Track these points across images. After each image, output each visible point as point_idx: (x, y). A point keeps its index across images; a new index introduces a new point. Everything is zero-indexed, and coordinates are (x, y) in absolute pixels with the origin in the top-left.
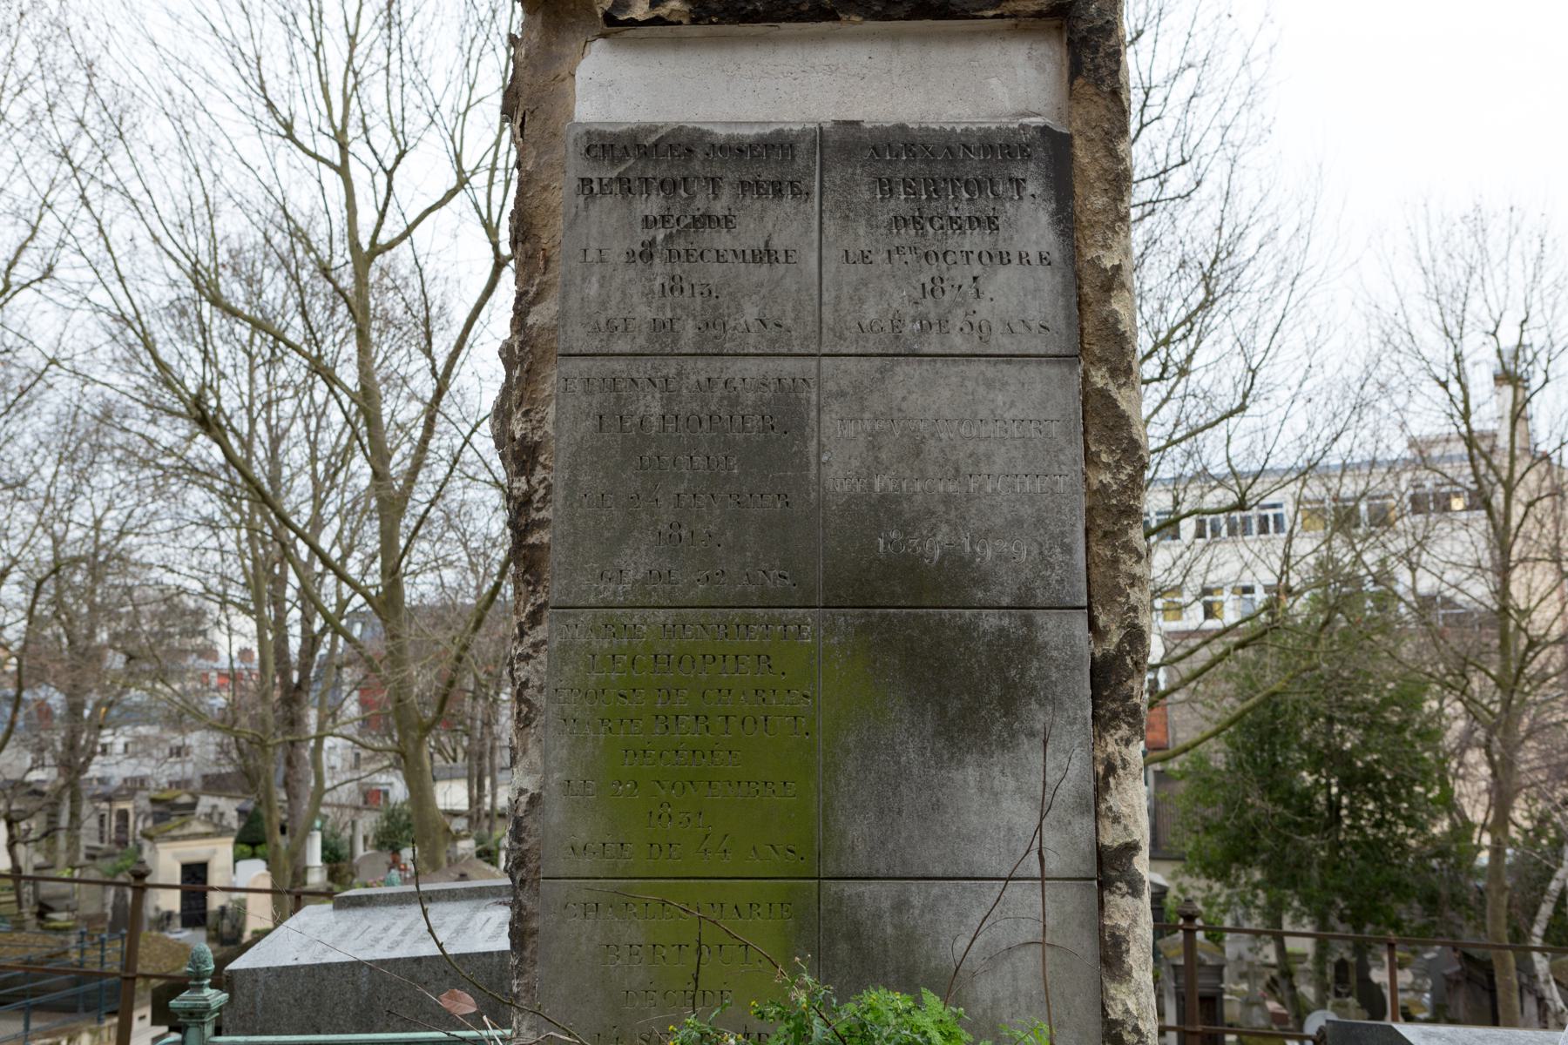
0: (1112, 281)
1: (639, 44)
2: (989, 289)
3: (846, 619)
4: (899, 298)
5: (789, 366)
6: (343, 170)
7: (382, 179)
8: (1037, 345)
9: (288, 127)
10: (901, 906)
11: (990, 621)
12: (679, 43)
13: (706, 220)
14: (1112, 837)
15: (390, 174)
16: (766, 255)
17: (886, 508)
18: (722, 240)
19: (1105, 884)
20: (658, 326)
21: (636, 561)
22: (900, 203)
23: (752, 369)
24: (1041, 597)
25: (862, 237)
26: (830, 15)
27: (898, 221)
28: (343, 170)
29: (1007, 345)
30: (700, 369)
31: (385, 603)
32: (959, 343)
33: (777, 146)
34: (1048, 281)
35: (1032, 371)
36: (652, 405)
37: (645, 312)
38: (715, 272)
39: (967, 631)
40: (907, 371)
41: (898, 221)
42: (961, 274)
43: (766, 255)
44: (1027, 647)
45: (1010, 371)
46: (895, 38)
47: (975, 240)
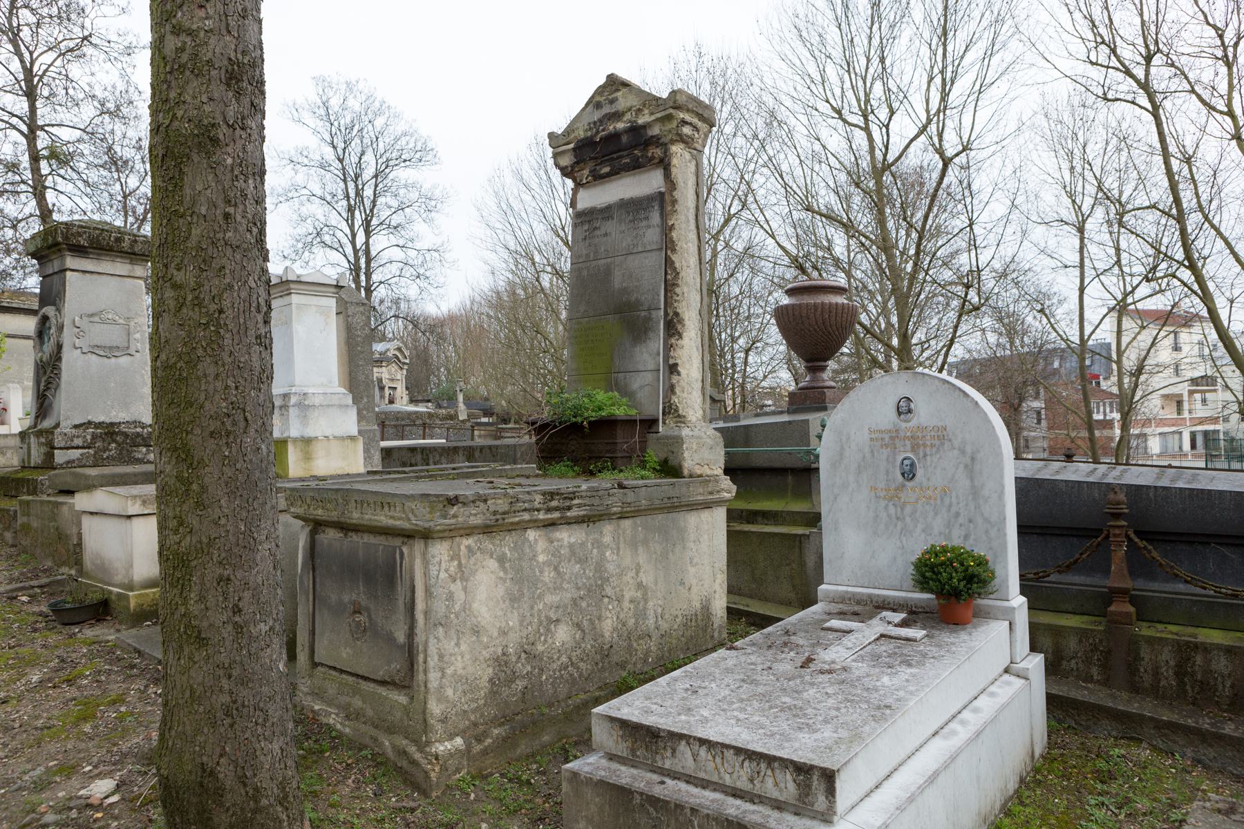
0: (672, 228)
1: (588, 187)
2: (646, 235)
3: (617, 316)
4: (629, 240)
5: (609, 260)
6: (867, 130)
7: (884, 130)
8: (655, 247)
9: (839, 112)
10: (625, 378)
11: (643, 314)
12: (595, 185)
13: (596, 228)
14: (671, 362)
15: (887, 127)
16: (606, 235)
17: (625, 291)
18: (598, 233)
19: (672, 373)
20: (587, 255)
21: (582, 308)
22: (631, 217)
23: (603, 261)
24: (653, 307)
25: (623, 227)
26: (618, 173)
27: (630, 221)
28: (867, 130)
29: (649, 248)
30: (594, 263)
31: (901, 351)
32: (640, 249)
33: (609, 208)
34: (658, 230)
35: (654, 253)
36: (585, 273)
37: (584, 252)
38: (597, 240)
39: (639, 316)
40: (630, 257)
41: (630, 221)
42: (641, 233)
43: (606, 235)
44: (648, 319)
45: (649, 254)
46: (634, 174)
47: (644, 223)
